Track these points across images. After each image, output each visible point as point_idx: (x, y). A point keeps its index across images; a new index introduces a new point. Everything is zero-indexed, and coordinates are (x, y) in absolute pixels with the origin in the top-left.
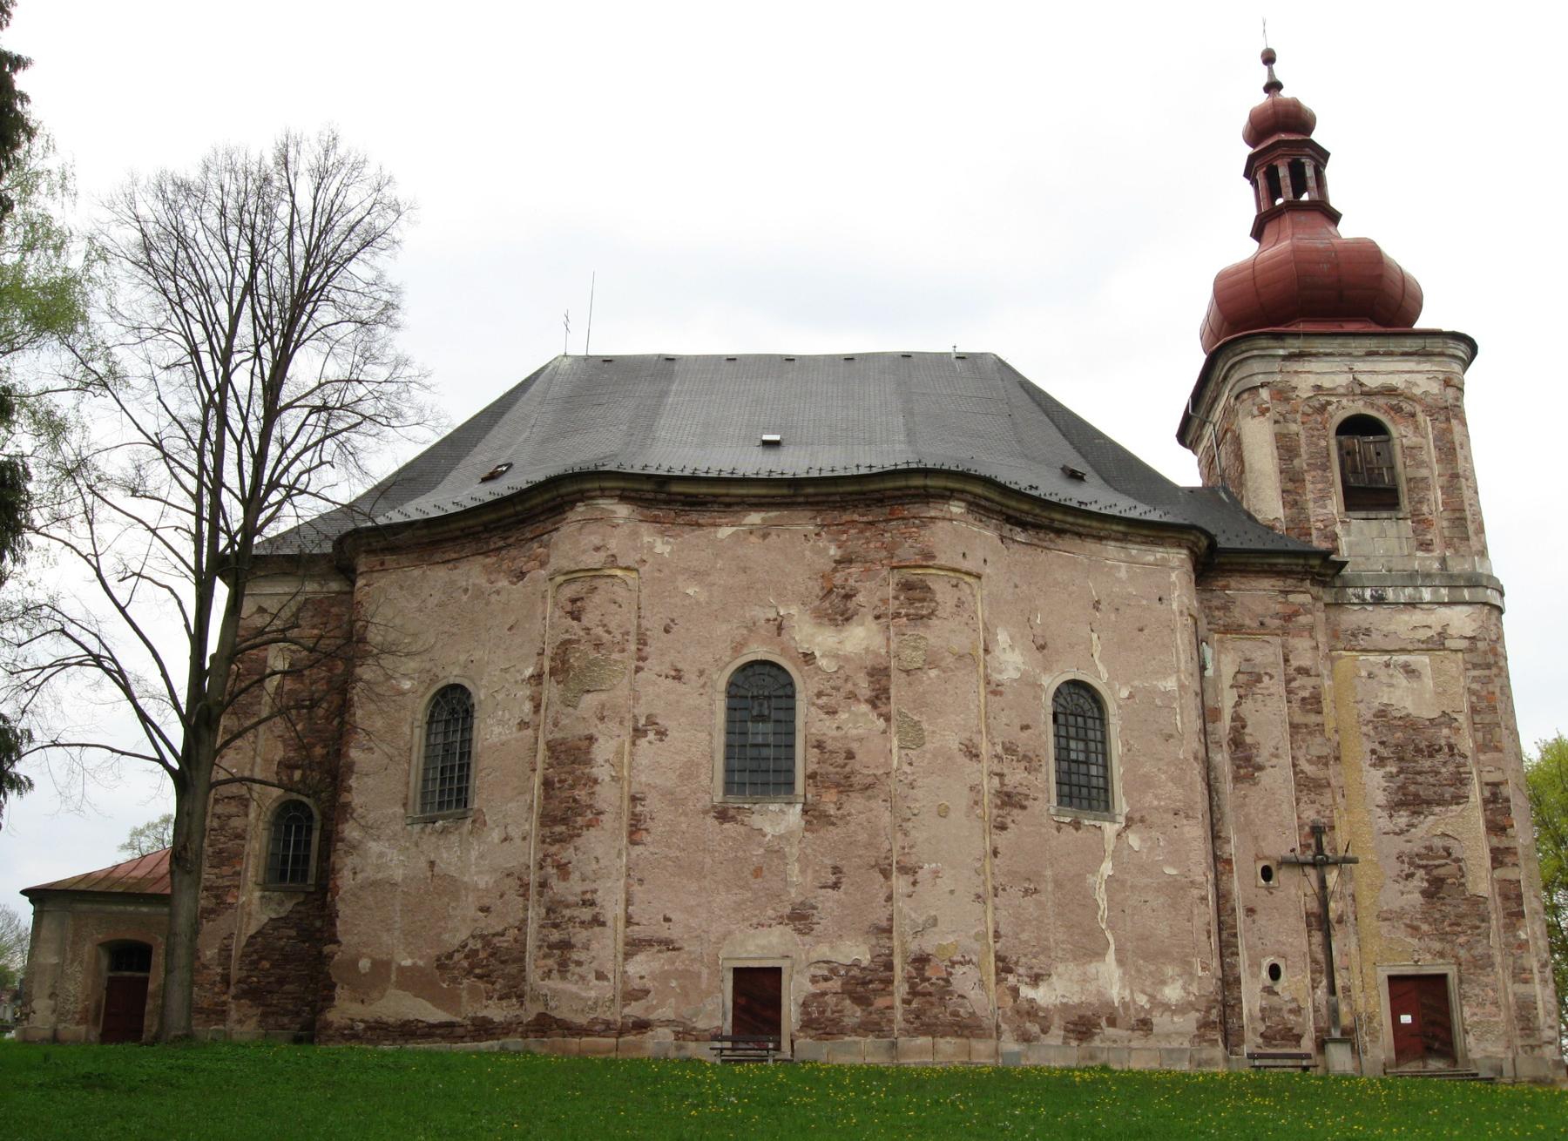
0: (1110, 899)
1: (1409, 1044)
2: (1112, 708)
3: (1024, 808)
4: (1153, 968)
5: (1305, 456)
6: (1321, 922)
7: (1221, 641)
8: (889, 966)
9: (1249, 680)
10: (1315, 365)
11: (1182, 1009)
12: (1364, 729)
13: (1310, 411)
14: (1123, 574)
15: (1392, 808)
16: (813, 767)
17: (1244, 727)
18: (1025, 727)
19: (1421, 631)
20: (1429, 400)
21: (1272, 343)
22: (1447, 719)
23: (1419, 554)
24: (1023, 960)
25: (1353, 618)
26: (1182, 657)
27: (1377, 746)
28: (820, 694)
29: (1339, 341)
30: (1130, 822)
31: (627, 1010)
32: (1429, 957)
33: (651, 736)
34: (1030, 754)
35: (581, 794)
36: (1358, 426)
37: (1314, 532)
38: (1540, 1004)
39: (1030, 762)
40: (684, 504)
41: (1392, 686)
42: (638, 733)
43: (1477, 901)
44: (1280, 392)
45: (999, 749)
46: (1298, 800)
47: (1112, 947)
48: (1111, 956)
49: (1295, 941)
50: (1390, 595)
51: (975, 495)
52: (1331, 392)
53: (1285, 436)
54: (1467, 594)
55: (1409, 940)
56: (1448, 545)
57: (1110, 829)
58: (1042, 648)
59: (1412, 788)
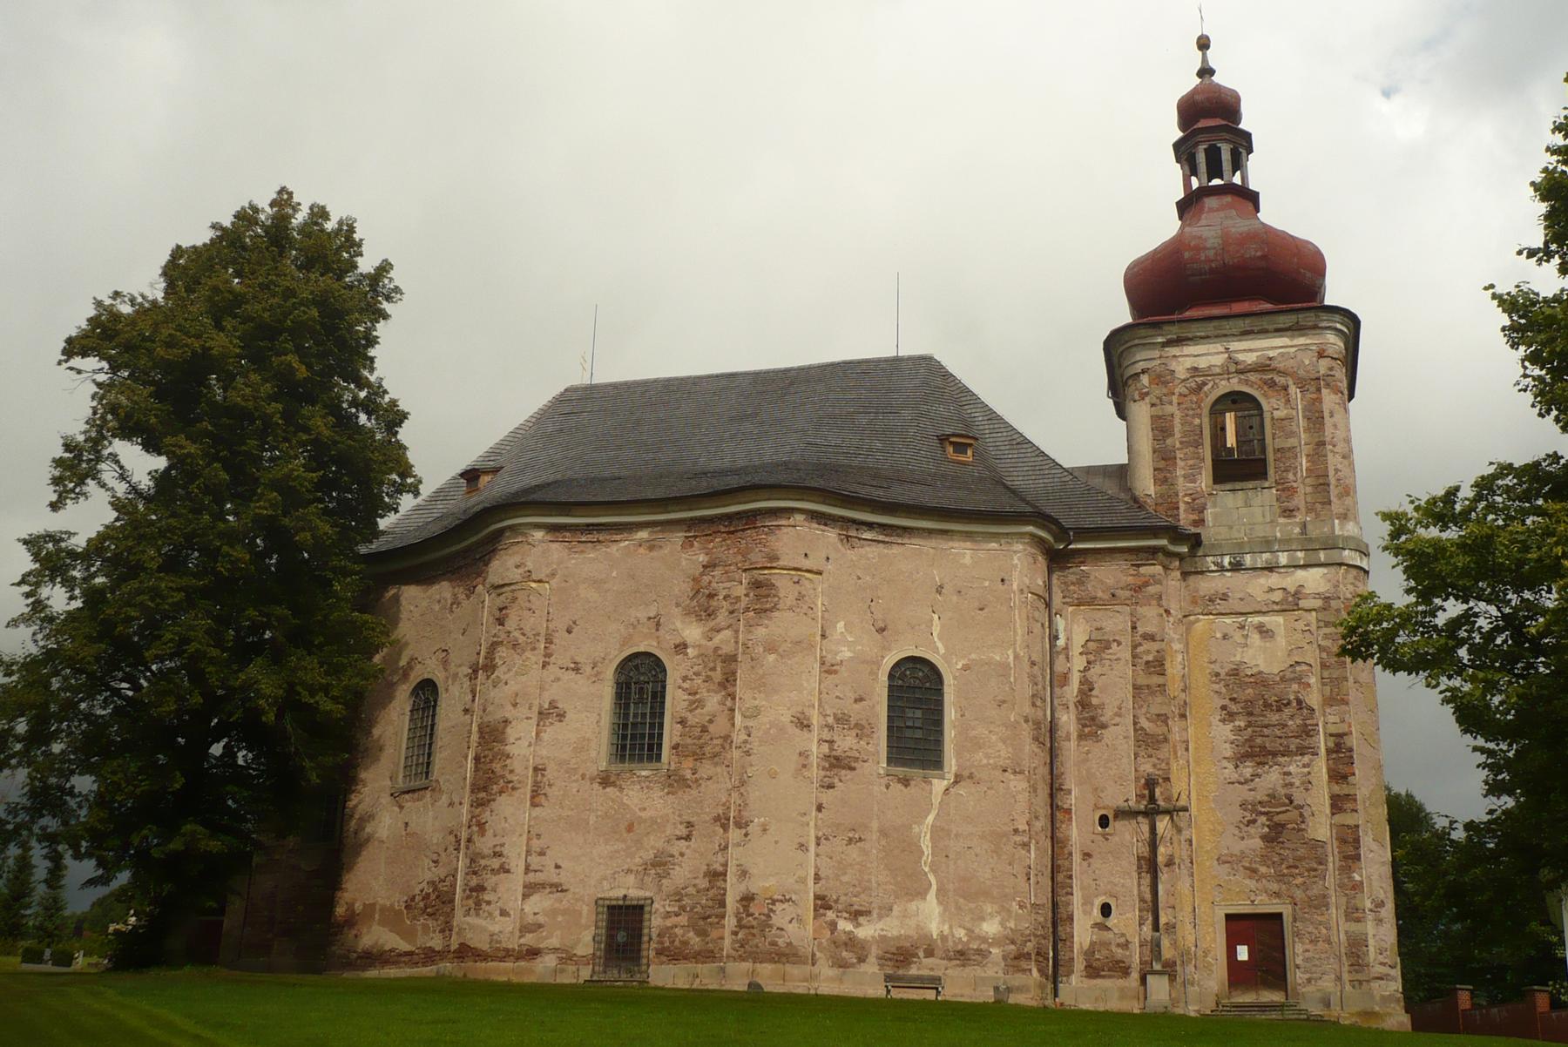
1: (1238, 975)
2: (948, 680)
4: (972, 906)
5: (1178, 435)
6: (1150, 866)
8: (723, 904)
9: (1099, 647)
11: (997, 942)
12: (1216, 687)
13: (1186, 391)
14: (967, 560)
16: (676, 739)
18: (859, 700)
20: (1301, 372)
21: (1151, 332)
22: (1294, 674)
23: (1282, 520)
25: (1208, 585)
27: (1226, 702)
28: (685, 679)
31: (522, 941)
32: (1264, 897)
34: (864, 722)
35: (497, 766)
36: (1235, 400)
37: (1182, 506)
38: (1371, 942)
39: (863, 731)
43: (1317, 844)
44: (1159, 376)
45: (830, 720)
46: (1136, 755)
47: (934, 887)
49: (1127, 884)
50: (1248, 560)
52: (1207, 373)
53: (1160, 417)
54: (1322, 556)
55: (1247, 881)
56: (1309, 510)
57: (939, 785)
58: (881, 630)
59: (1259, 741)
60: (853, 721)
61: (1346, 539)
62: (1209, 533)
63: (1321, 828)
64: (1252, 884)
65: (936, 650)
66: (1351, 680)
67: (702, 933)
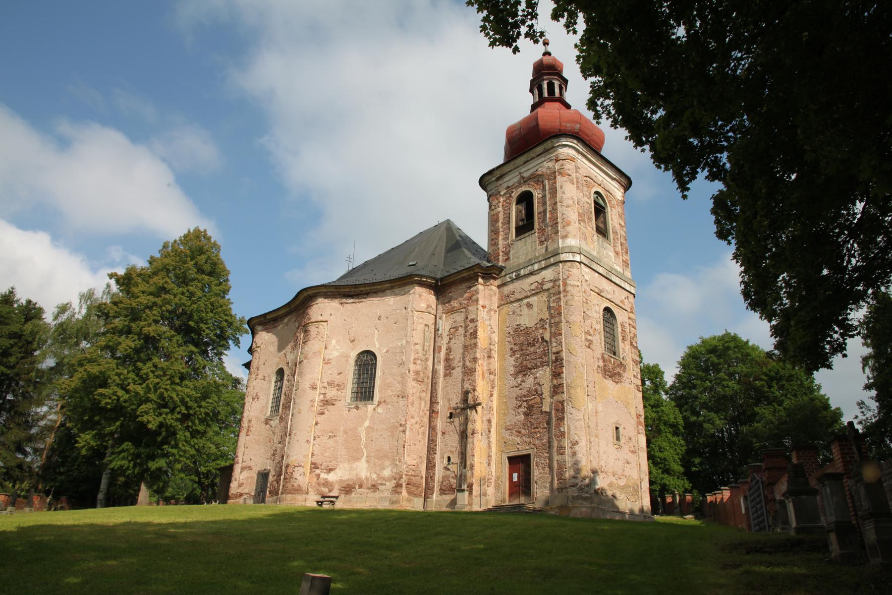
3: (333, 405)
5: (501, 221)
6: (464, 436)
10: (507, 179)
11: (389, 479)
12: (509, 339)
14: (392, 303)
27: (513, 346)
30: (379, 403)
37: (501, 254)
39: (339, 387)
42: (253, 399)
45: (325, 384)
54: (552, 260)
57: (370, 407)
58: (352, 341)
64: (518, 440)
67: (278, 483)
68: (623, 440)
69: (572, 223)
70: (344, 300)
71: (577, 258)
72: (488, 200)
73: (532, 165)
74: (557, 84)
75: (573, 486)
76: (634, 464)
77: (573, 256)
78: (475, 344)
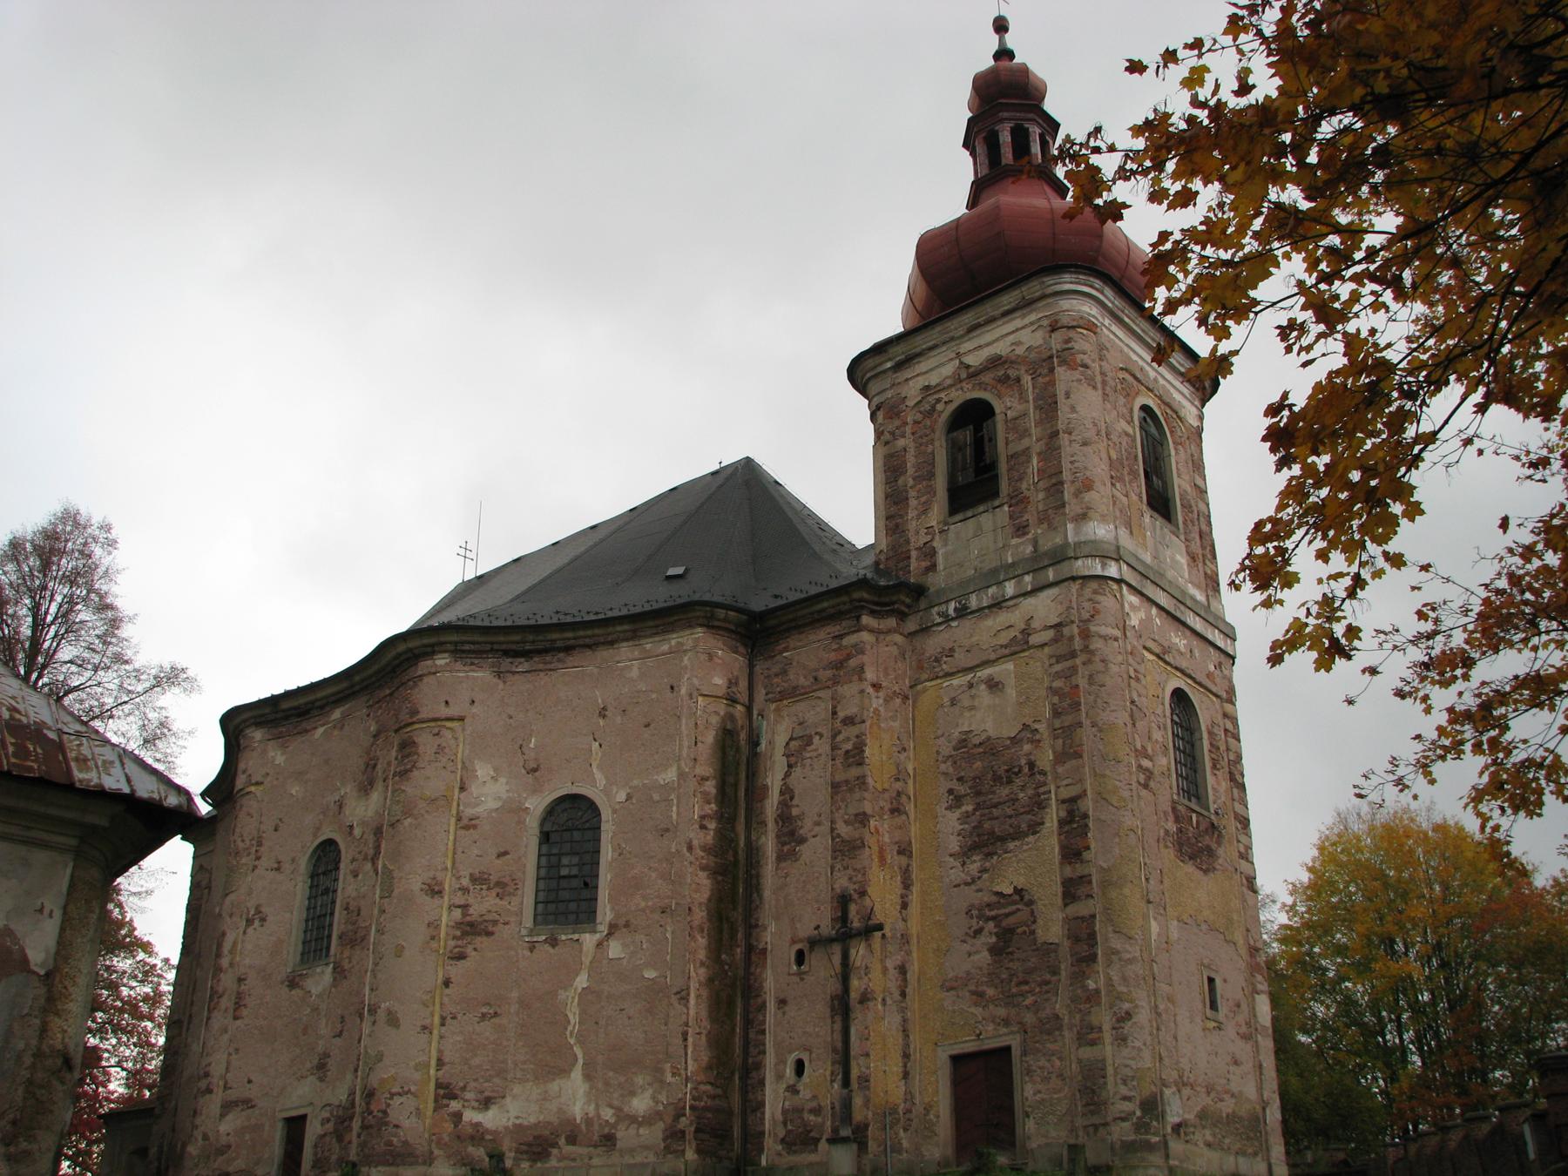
0: (583, 1012)
2: (606, 814)
3: (492, 934)
4: (622, 1079)
5: (911, 471)
6: (842, 1007)
7: (777, 710)
10: (923, 366)
11: (648, 1120)
12: (943, 767)
13: (919, 417)
14: (635, 673)
15: (965, 854)
17: (792, 798)
18: (501, 855)
19: (1003, 634)
21: (878, 359)
23: (1014, 541)
24: (473, 1084)
26: (686, 744)
27: (955, 785)
29: (938, 328)
30: (613, 929)
32: (991, 1027)
33: (257, 923)
37: (914, 554)
38: (1110, 1070)
39: (503, 888)
40: (299, 715)
41: (972, 708)
42: (250, 922)
43: (1049, 949)
45: (465, 882)
46: (832, 868)
47: (581, 1061)
48: (577, 1074)
50: (973, 602)
51: (456, 643)
54: (1051, 574)
55: (973, 1010)
56: (1041, 521)
57: (589, 940)
59: (986, 826)
60: (493, 878)
61: (1078, 544)
62: (937, 581)
63: (1052, 927)
64: (977, 1011)
65: (594, 783)
66: (1086, 722)
67: (340, 1139)
68: (1223, 1009)
69: (1097, 485)
70: (506, 663)
71: (1113, 570)
72: (873, 417)
73: (988, 338)
74: (1035, 131)
75: (1123, 1119)
76: (1248, 1066)
77: (1104, 566)
78: (861, 781)
